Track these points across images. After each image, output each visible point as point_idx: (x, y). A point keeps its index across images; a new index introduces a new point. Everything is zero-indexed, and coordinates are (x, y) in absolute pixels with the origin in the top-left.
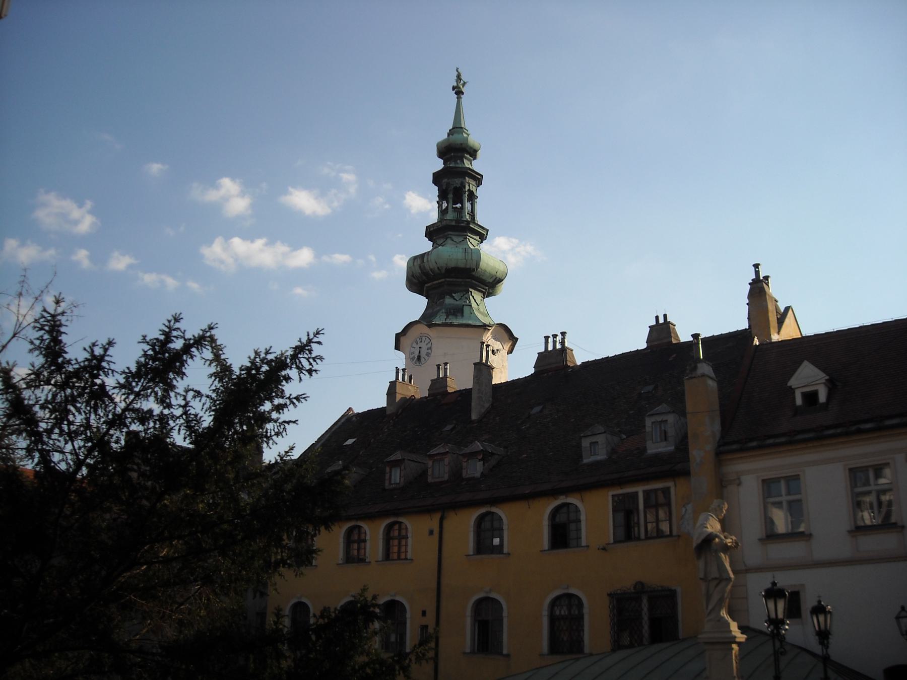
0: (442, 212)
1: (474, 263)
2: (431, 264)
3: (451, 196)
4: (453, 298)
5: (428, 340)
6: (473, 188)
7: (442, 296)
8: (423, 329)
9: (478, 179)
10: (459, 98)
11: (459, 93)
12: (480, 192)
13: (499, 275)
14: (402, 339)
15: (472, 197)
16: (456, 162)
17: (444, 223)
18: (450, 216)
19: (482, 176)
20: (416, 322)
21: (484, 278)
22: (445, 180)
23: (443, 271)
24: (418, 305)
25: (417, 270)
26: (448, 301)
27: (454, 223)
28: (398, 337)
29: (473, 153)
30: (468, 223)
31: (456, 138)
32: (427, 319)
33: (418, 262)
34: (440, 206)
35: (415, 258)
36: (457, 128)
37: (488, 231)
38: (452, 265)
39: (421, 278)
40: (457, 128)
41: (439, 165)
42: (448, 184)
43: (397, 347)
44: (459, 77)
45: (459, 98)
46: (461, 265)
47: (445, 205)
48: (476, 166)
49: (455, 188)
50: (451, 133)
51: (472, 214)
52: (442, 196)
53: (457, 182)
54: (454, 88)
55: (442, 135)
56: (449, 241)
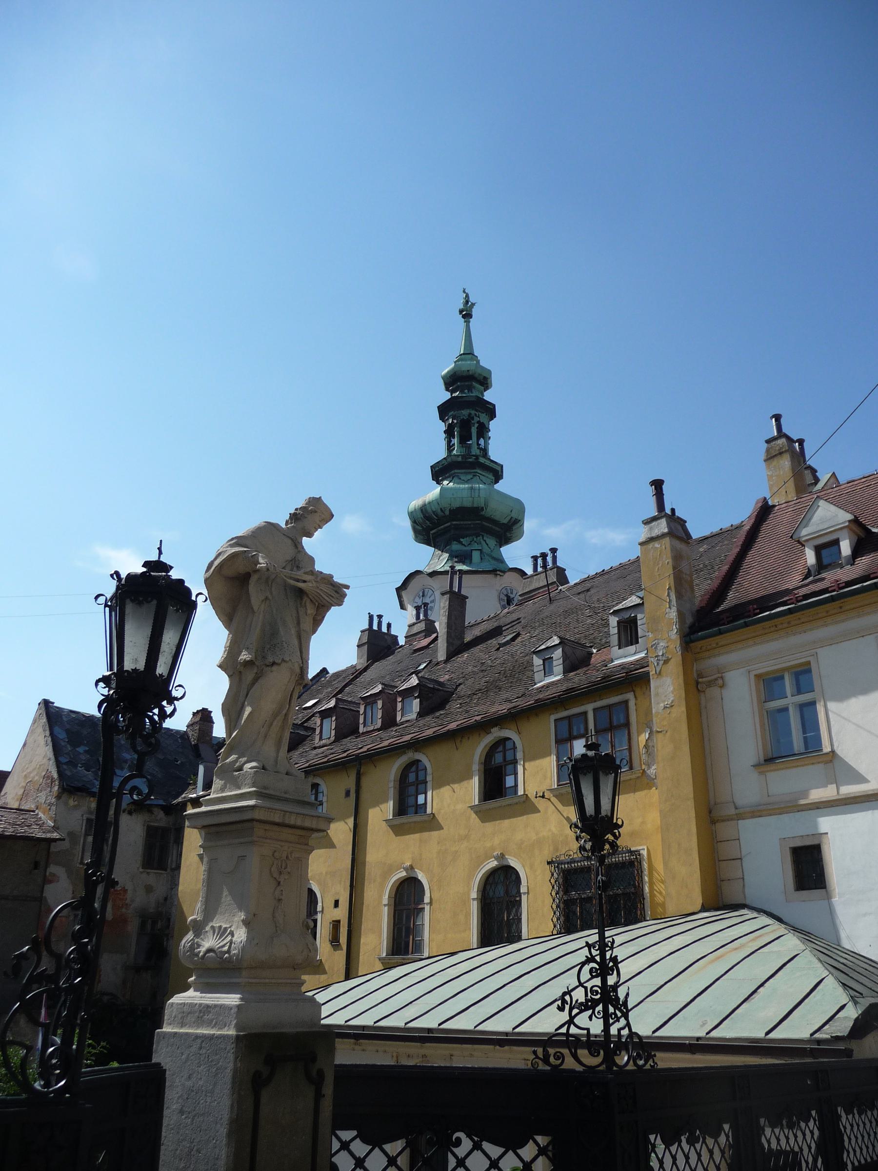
0: (450, 447)
9: (490, 411)
10: (468, 323)
11: (467, 314)
12: (493, 425)
13: (514, 515)
14: (404, 593)
15: (483, 431)
17: (449, 460)
19: (494, 406)
20: (418, 572)
21: (497, 518)
23: (447, 513)
24: (427, 558)
25: (420, 515)
26: (455, 546)
27: (460, 459)
28: (399, 590)
29: (485, 382)
30: (477, 457)
36: (469, 353)
37: (502, 466)
38: (456, 504)
39: (430, 526)
40: (469, 353)
41: (447, 396)
43: (402, 607)
45: (468, 323)
46: (467, 504)
48: (488, 396)
51: (485, 452)
52: (449, 433)
53: (465, 413)
54: (461, 312)
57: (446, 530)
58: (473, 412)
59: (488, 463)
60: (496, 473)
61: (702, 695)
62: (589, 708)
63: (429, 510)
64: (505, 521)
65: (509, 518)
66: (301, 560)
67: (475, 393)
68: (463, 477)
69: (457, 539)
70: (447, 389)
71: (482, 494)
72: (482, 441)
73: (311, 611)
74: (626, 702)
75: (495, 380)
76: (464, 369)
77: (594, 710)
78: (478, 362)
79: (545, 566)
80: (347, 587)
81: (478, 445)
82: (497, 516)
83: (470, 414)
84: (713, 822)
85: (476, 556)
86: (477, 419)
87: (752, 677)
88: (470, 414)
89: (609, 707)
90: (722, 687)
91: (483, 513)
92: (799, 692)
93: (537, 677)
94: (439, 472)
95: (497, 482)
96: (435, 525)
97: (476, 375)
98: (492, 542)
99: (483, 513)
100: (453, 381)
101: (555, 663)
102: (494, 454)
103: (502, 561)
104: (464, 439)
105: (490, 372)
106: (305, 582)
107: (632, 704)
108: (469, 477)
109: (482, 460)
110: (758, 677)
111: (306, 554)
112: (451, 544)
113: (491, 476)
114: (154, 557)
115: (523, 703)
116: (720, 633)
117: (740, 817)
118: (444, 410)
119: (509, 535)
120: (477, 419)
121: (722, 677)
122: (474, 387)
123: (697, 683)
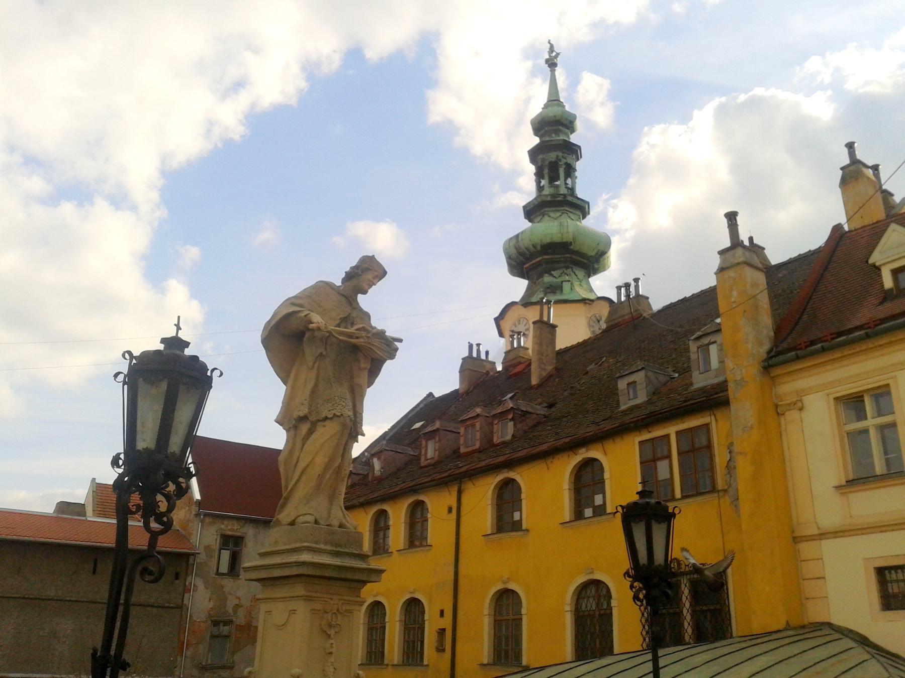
0: (540, 188)
1: (571, 237)
2: (526, 243)
3: (546, 171)
4: (552, 275)
5: (525, 321)
6: (569, 161)
7: (541, 276)
8: (520, 311)
12: (579, 165)
13: (601, 248)
14: (502, 323)
15: (570, 171)
16: (550, 136)
17: (539, 200)
18: (547, 191)
20: (513, 304)
22: (541, 156)
23: (539, 248)
25: (513, 251)
26: (547, 279)
27: (549, 199)
30: (565, 195)
31: (554, 111)
32: (526, 303)
33: (514, 241)
34: (538, 183)
35: (511, 239)
38: (547, 240)
40: (554, 100)
41: (536, 141)
42: (543, 160)
44: (552, 47)
46: (557, 239)
47: (543, 182)
48: (574, 138)
49: (551, 163)
50: (546, 106)
51: (572, 190)
52: (539, 175)
53: (552, 156)
55: (536, 108)
56: (546, 218)
57: (539, 264)
58: (560, 154)
59: (575, 201)
60: (581, 208)
61: (782, 418)
62: (671, 430)
63: (523, 247)
64: (593, 254)
65: (596, 251)
66: (353, 315)
67: (562, 137)
68: (552, 214)
69: (549, 272)
70: (536, 134)
71: (571, 230)
72: (569, 181)
73: (365, 364)
74: (707, 425)
75: (578, 124)
76: (551, 115)
77: (677, 433)
78: (564, 107)
79: (628, 296)
80: (400, 341)
81: (566, 184)
82: (585, 250)
83: (558, 156)
84: (796, 540)
85: (566, 287)
86: (564, 161)
87: (832, 402)
88: (558, 156)
89: (691, 429)
90: (801, 409)
91: (571, 247)
92: (880, 414)
93: (622, 399)
94: (532, 212)
95: (584, 217)
96: (528, 259)
97: (562, 120)
98: (581, 273)
99: (571, 247)
100: (542, 126)
101: (638, 387)
102: (581, 193)
103: (591, 290)
104: (553, 178)
105: (575, 117)
106: (357, 338)
107: (714, 425)
108: (558, 214)
109: (569, 198)
110: (836, 399)
111: (361, 310)
112: (542, 277)
113: (578, 213)
114: (171, 333)
115: (607, 426)
116: (798, 358)
117: (823, 535)
118: (534, 154)
119: (596, 266)
120: (564, 161)
121: (801, 400)
122: (561, 131)
123: (777, 406)
